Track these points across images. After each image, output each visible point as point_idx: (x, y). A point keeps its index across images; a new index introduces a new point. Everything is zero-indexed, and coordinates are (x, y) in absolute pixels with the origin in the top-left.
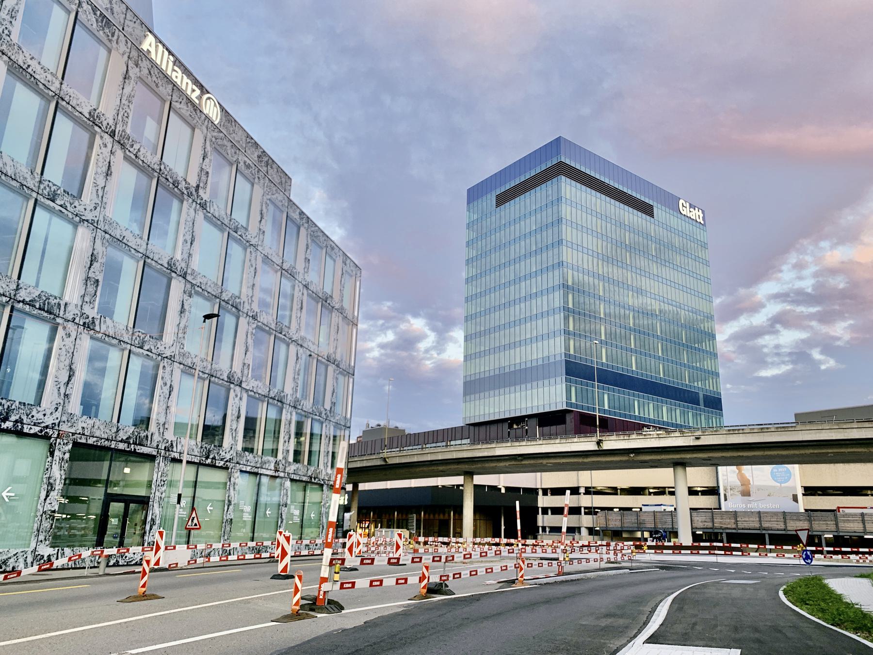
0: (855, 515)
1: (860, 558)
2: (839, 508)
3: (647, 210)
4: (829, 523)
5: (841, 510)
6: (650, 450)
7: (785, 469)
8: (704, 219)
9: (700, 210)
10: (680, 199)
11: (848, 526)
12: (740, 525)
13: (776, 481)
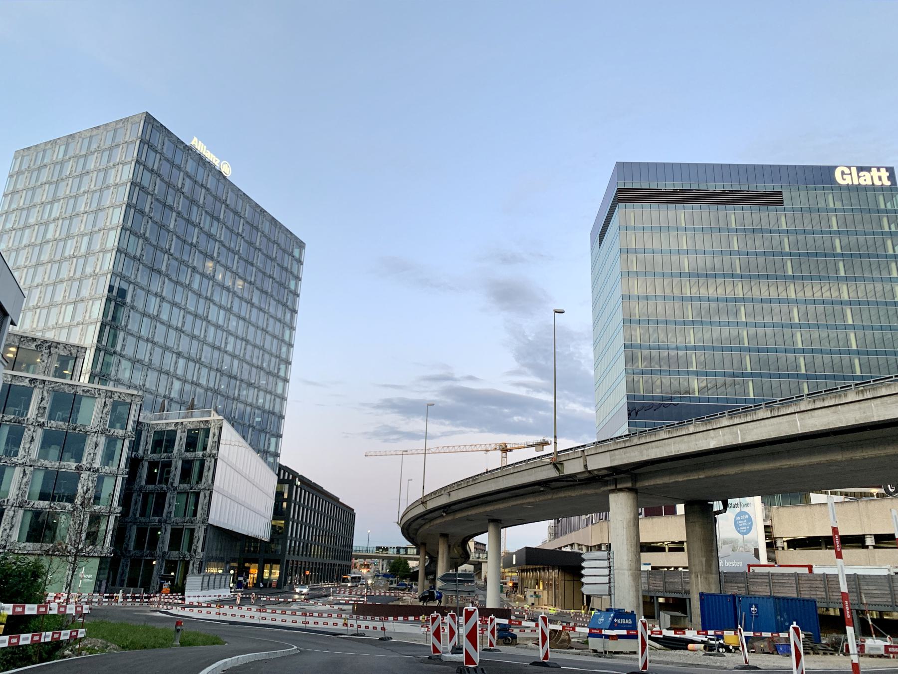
0: (763, 574)
1: (661, 633)
2: (749, 566)
3: (774, 199)
4: (739, 585)
5: (751, 568)
6: (464, 505)
7: (747, 516)
8: (891, 177)
9: (881, 169)
10: (836, 167)
11: (761, 590)
12: (670, 587)
13: (739, 532)
